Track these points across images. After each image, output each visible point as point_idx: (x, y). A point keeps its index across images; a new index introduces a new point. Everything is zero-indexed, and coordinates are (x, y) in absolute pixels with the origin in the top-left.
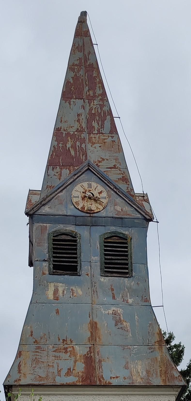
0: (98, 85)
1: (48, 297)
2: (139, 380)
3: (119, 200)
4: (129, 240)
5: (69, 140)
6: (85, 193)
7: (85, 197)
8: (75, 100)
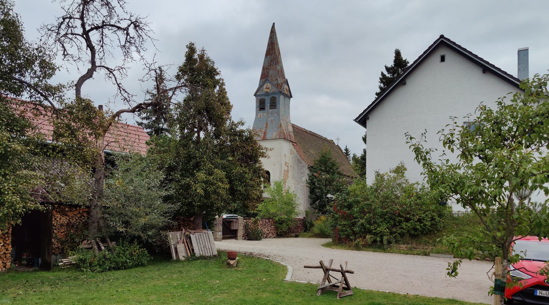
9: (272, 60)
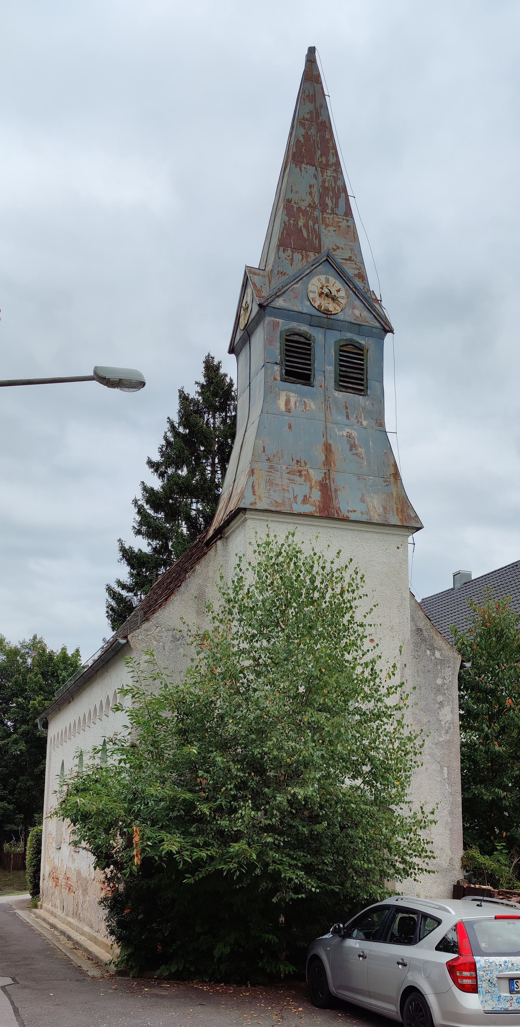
0: (331, 151)
1: (279, 408)
2: (377, 517)
3: (357, 303)
4: (365, 351)
5: (301, 217)
6: (322, 288)
7: (323, 293)
8: (306, 166)
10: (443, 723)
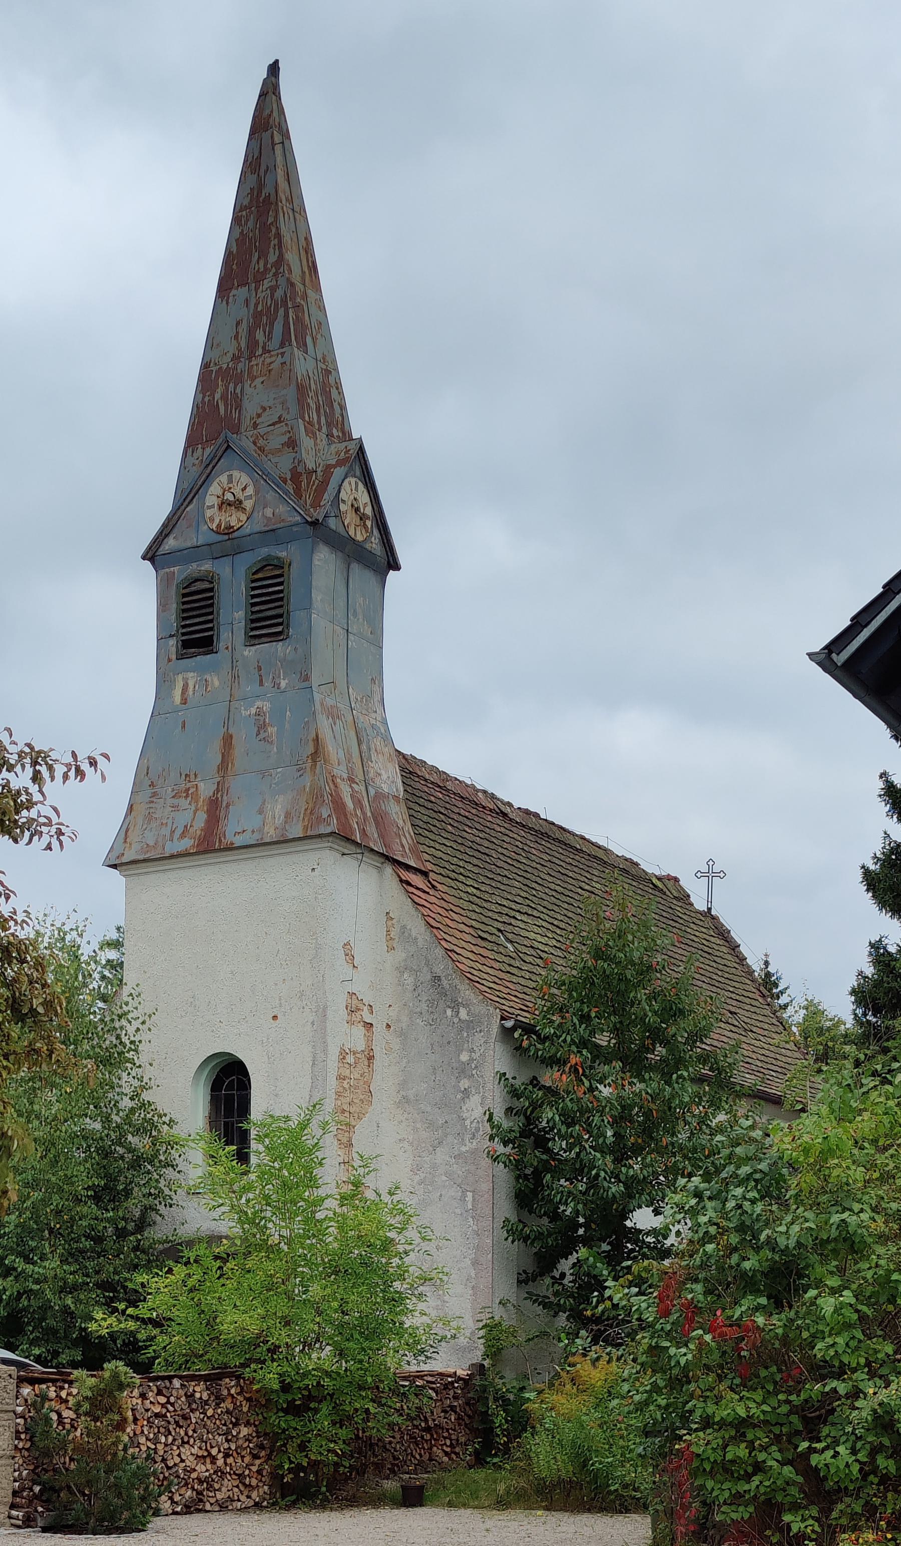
0: (272, 243)
5: (220, 383)
9: (261, 318)
10: (468, 1122)
